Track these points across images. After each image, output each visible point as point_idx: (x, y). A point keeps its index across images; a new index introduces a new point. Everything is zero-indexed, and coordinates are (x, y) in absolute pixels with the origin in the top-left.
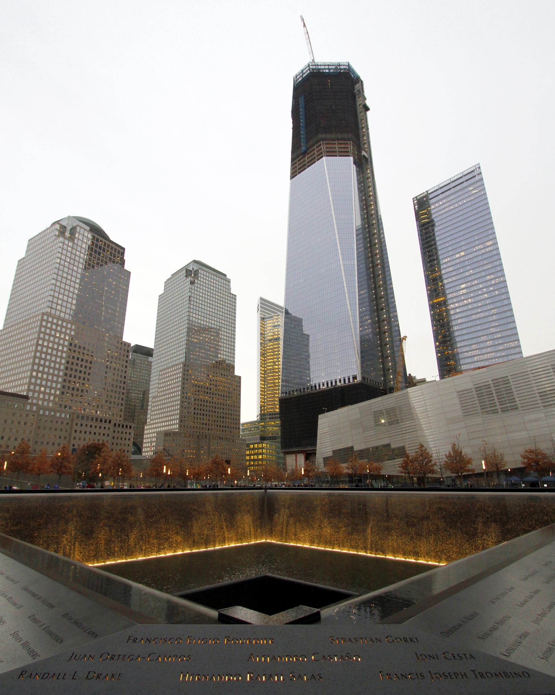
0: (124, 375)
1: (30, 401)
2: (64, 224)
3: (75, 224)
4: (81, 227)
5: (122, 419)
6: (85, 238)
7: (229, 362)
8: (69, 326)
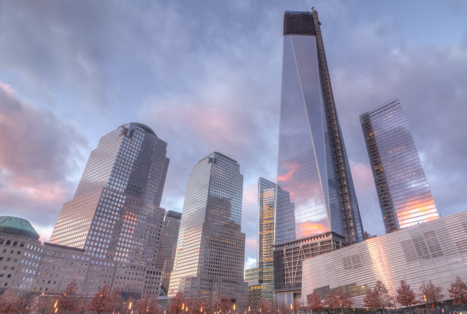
0: (158, 232)
1: (85, 253)
2: (128, 127)
3: (134, 128)
4: (138, 129)
5: (154, 267)
6: (140, 136)
7: (237, 223)
8: (122, 196)
